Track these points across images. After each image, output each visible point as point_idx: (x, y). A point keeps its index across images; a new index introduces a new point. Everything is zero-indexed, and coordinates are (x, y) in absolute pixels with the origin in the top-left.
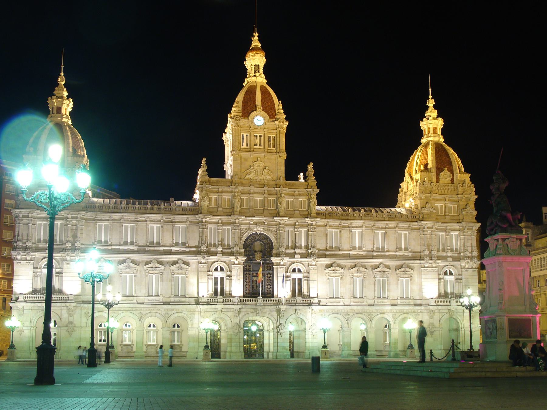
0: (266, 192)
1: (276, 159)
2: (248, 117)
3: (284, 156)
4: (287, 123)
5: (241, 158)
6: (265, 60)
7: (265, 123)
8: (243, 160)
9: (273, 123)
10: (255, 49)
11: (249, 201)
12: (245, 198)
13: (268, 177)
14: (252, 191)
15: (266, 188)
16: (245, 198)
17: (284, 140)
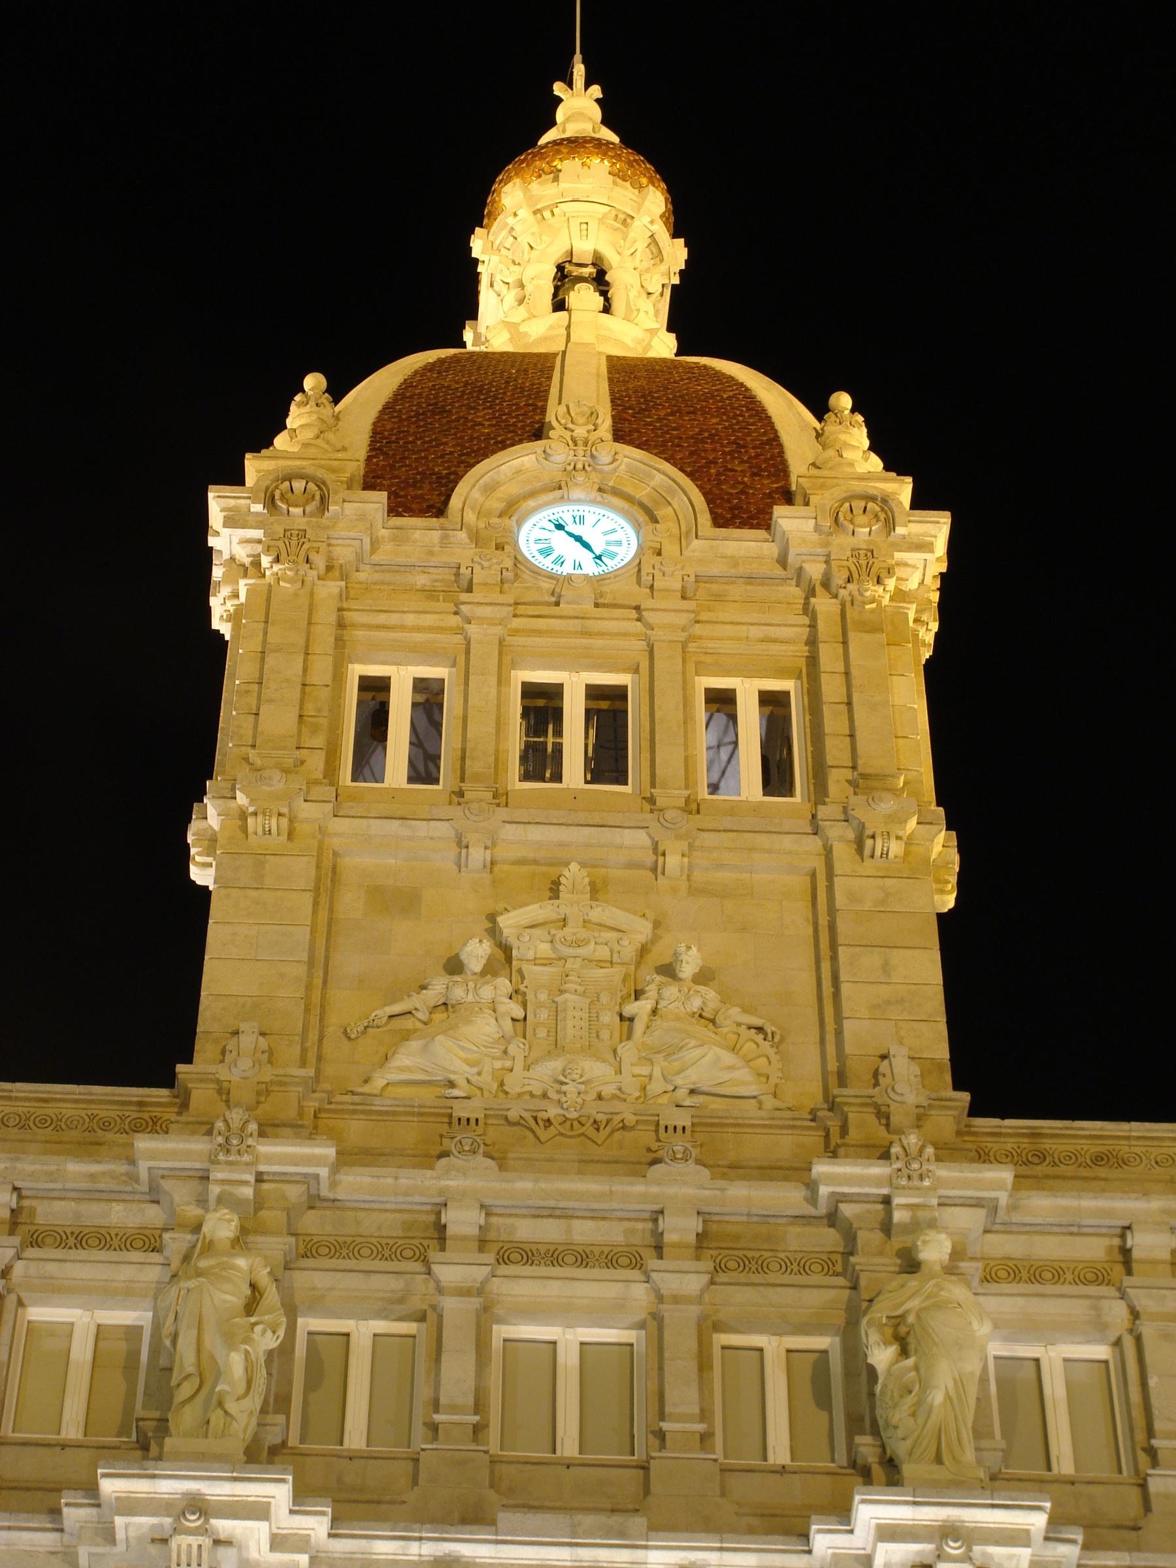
0: (680, 1228)
1: (820, 888)
2: (439, 510)
3: (920, 859)
4: (937, 529)
5: (328, 880)
6: (677, 253)
7: (651, 551)
8: (351, 903)
9: (744, 544)
10: (575, 145)
11: (409, 1368)
12: (363, 1331)
13: (713, 1066)
14: (462, 1221)
15: (682, 1192)
16: (363, 1331)
17: (910, 700)
